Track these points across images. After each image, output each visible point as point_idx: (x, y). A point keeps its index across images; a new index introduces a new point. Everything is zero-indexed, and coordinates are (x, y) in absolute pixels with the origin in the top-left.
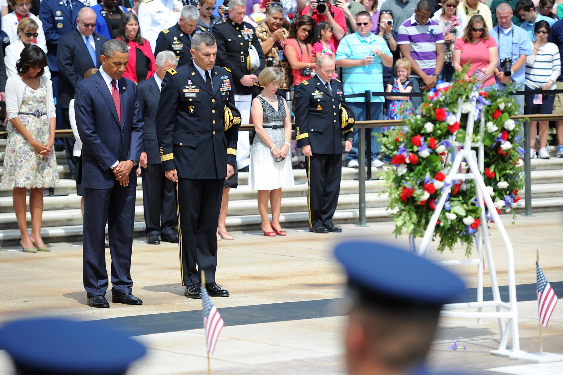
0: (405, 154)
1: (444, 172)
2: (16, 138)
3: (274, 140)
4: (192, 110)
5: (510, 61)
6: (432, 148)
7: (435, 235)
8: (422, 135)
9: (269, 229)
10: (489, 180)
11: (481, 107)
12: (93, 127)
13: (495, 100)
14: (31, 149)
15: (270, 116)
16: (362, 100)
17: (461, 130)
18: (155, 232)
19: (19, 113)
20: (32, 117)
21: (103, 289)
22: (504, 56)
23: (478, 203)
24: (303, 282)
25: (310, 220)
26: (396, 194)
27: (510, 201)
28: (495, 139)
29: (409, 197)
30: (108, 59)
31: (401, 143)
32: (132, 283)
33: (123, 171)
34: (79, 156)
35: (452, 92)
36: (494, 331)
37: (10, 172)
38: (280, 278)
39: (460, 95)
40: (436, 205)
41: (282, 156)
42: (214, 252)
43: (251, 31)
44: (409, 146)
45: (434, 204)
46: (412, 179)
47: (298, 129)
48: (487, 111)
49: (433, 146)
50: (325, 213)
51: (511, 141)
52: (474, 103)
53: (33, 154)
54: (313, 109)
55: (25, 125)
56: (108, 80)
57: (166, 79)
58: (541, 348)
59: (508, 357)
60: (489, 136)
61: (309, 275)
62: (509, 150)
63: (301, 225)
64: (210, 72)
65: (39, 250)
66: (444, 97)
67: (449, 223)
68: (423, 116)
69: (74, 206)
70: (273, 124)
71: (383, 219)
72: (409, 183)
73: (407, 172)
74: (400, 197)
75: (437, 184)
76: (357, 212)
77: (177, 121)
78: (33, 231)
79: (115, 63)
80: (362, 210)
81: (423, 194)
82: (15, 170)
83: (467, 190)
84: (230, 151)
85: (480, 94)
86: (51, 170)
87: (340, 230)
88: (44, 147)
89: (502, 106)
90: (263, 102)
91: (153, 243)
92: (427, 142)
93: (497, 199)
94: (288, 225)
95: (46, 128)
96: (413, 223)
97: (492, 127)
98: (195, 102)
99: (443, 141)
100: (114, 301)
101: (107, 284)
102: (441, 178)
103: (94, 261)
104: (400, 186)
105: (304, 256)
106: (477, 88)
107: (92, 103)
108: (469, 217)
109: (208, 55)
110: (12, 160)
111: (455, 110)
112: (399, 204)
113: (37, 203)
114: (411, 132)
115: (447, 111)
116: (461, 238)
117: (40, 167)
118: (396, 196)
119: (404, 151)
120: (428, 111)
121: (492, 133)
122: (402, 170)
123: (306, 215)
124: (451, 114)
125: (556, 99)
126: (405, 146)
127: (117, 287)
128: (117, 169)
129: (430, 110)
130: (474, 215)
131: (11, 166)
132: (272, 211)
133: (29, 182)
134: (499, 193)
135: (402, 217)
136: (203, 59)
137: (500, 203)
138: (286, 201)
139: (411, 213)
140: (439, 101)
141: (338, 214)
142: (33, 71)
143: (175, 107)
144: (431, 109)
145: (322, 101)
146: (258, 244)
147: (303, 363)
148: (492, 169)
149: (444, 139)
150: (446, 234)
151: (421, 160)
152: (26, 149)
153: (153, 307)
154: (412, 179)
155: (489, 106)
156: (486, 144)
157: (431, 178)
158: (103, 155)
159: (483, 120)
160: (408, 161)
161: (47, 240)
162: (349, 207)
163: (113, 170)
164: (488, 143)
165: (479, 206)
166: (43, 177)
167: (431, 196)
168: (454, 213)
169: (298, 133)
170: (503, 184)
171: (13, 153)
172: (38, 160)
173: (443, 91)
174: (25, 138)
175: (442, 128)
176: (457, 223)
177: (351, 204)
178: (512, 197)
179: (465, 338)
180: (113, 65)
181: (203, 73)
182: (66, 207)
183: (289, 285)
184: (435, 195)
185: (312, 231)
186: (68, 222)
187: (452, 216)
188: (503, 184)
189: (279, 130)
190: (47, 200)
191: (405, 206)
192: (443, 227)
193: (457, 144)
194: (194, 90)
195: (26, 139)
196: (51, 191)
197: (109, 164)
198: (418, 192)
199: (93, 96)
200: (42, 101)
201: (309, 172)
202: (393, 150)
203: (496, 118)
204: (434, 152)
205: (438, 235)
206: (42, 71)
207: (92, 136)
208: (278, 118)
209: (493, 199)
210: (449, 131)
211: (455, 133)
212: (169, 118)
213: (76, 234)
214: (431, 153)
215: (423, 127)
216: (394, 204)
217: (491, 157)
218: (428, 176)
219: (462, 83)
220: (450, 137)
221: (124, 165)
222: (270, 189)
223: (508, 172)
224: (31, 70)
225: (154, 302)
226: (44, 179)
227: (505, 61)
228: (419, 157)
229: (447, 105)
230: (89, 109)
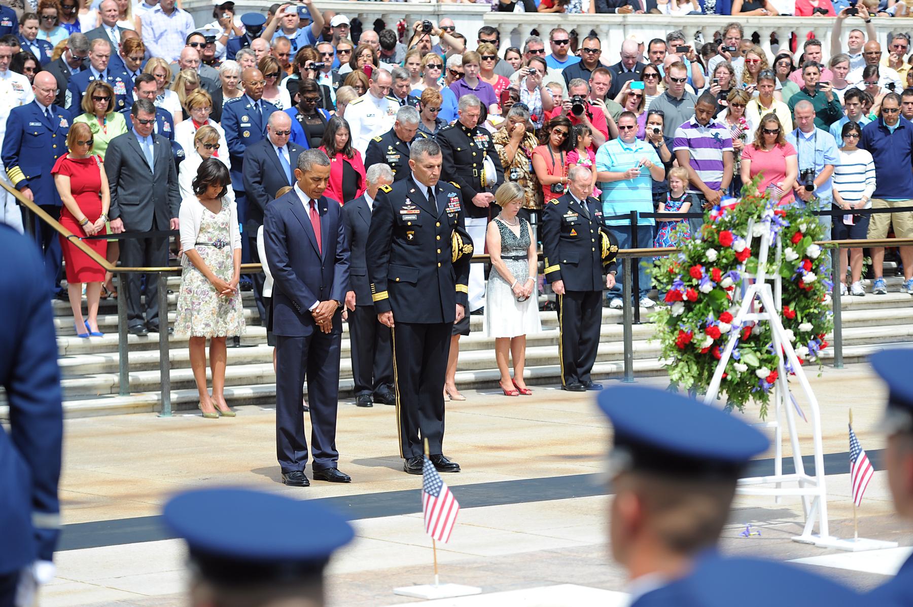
0: (681, 289)
1: (731, 311)
3: (515, 274)
4: (411, 237)
5: (813, 173)
6: (716, 281)
7: (721, 392)
8: (703, 264)
9: (509, 387)
10: (789, 322)
11: (777, 229)
12: (286, 259)
13: (795, 220)
15: (510, 244)
16: (626, 222)
17: (752, 258)
18: (366, 392)
19: (196, 244)
20: (213, 248)
21: (301, 462)
22: (804, 166)
23: (775, 351)
24: (554, 453)
25: (562, 375)
26: (671, 340)
27: (815, 348)
28: (795, 270)
29: (687, 343)
30: (304, 174)
31: (676, 274)
32: (337, 455)
33: (324, 314)
34: (270, 296)
35: (740, 210)
36: (796, 513)
37: (185, 318)
38: (524, 447)
39: (751, 214)
40: (721, 353)
41: (526, 294)
42: (439, 413)
44: (687, 279)
45: (719, 352)
46: (690, 320)
47: (546, 259)
48: (785, 234)
49: (717, 278)
50: (581, 365)
51: (815, 272)
52: (768, 224)
53: (213, 294)
56: (304, 200)
57: (379, 198)
58: (856, 535)
59: (814, 544)
60: (788, 265)
61: (561, 444)
62: (813, 283)
63: (551, 381)
64: (433, 188)
65: (222, 415)
66: (730, 217)
67: (739, 376)
68: (704, 241)
69: (265, 359)
70: (513, 254)
71: (655, 373)
72: (688, 325)
73: (684, 312)
74: (676, 343)
75: (723, 327)
76: (622, 364)
77: (392, 250)
78: (215, 391)
79: (313, 179)
80: (628, 362)
81: (705, 340)
82: (192, 315)
83: (761, 333)
84: (460, 288)
85: (776, 213)
86: (235, 314)
88: (228, 286)
89: (803, 228)
90: (502, 227)
91: (365, 405)
92: (709, 275)
93: (799, 345)
94: (534, 381)
95: (229, 262)
96: (693, 376)
97: (791, 254)
98: (415, 226)
99: (729, 272)
100: (316, 478)
101: (306, 457)
102: (728, 319)
103: (290, 427)
104: (675, 329)
105: (556, 421)
106: (772, 205)
107: (285, 229)
108: (764, 368)
109: (431, 167)
111: (745, 234)
112: (675, 352)
113: (219, 355)
114: (689, 260)
115: (734, 234)
116: (754, 395)
117: (223, 311)
118: (671, 342)
119: (680, 285)
120: (710, 235)
121: (791, 262)
122: (678, 309)
123: (557, 369)
124: (739, 238)
125: (871, 220)
126: (680, 279)
127: (319, 461)
128: (318, 311)
129: (712, 233)
130: (769, 366)
132: (514, 364)
133: (209, 329)
134: (802, 338)
135: (678, 369)
136: (425, 172)
137: (803, 350)
138: (531, 352)
139: (689, 363)
140: (723, 222)
141: (597, 368)
142: (212, 191)
143: (390, 232)
144: (715, 231)
145: (577, 225)
147: (555, 555)
148: (792, 308)
149: (731, 269)
150: (734, 390)
151: (702, 297)
153: (364, 485)
154: (690, 320)
155: (787, 228)
156: (784, 276)
157: (715, 319)
158: (299, 293)
159: (779, 245)
160: (685, 298)
161: (232, 402)
162: (611, 358)
163: (312, 312)
164: (786, 274)
165: (776, 354)
166: (226, 323)
167: (714, 341)
168: (745, 363)
169: (547, 265)
170: (806, 327)
173: (729, 209)
174: (204, 275)
175: (729, 256)
176: (749, 376)
177: (614, 354)
178: (817, 343)
179: (760, 521)
180: (311, 181)
181: (424, 190)
182: (255, 361)
183: (536, 457)
184: (720, 341)
186: (258, 380)
187: (742, 368)
188: (806, 327)
189: (521, 262)
190: (232, 352)
191: (682, 355)
192: (731, 381)
193: (747, 276)
194: (413, 212)
196: (236, 341)
197: (306, 305)
198: (698, 336)
199: (286, 220)
200: (225, 228)
201: (561, 315)
202: (667, 284)
203: (796, 243)
204: (718, 287)
205: (724, 391)
206: (224, 191)
207: (286, 271)
208: (520, 246)
209: (794, 345)
210: (737, 259)
211: (744, 262)
212: (382, 247)
213: (268, 394)
214: (714, 288)
215: (704, 254)
216: (668, 352)
217: (791, 291)
218: (711, 316)
219: (753, 199)
220: (738, 266)
221: (326, 306)
222: (511, 336)
223: (812, 310)
224: (211, 190)
225: (366, 479)
227: (806, 173)
228: (700, 292)
229: (735, 226)
230: (281, 236)
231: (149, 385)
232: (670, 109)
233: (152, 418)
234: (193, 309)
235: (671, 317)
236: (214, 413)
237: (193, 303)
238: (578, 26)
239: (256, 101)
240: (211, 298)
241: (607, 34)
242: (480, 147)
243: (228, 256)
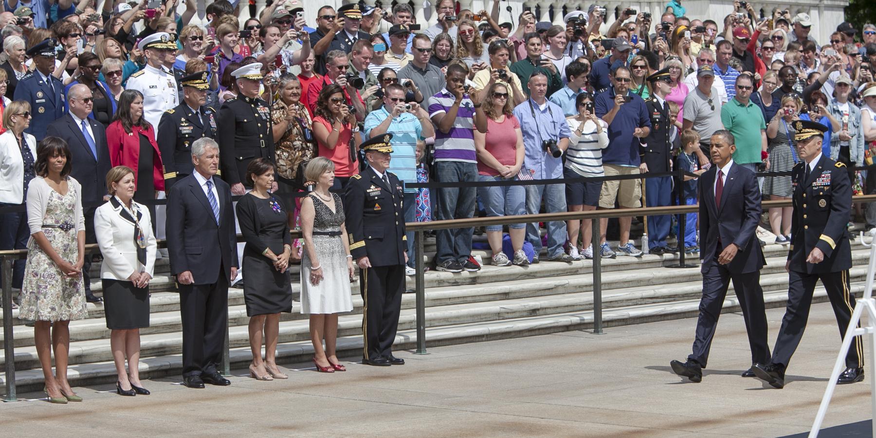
2: (40, 258)
9: (325, 363)
14: (57, 271)
15: (328, 220)
19: (43, 226)
20: (59, 230)
37: (30, 301)
43: (267, 110)
54: (370, 210)
55: (51, 241)
65: (69, 400)
69: (79, 337)
70: (330, 230)
71: (437, 343)
82: (37, 298)
86: (80, 298)
87: (400, 362)
88: (73, 268)
90: (317, 202)
110: (33, 286)
125: (603, 186)
131: (30, 293)
145: (381, 198)
146: (328, 384)
152: (52, 272)
166: (69, 307)
171: (34, 276)
172: (64, 286)
185: (368, 364)
195: (53, 259)
208: (336, 222)
222: (327, 312)
226: (71, 310)
234: (39, 292)
237: (39, 287)
240: (57, 281)
243: (73, 239)
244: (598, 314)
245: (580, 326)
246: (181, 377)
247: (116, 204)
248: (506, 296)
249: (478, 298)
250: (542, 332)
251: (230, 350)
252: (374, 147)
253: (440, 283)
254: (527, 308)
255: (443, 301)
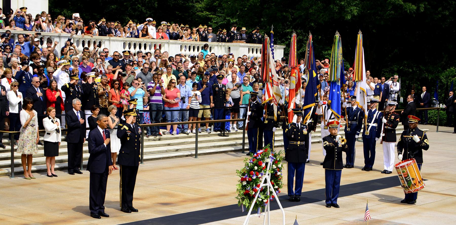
5: (185, 98)
6: (257, 175)
20: (31, 126)
22: (182, 96)
24: (157, 202)
37: (21, 148)
60: (273, 170)
65: (31, 178)
69: (35, 156)
75: (257, 188)
82: (23, 147)
90: (112, 119)
97: (274, 167)
102: (258, 186)
107: (95, 140)
121: (274, 169)
122: (245, 183)
133: (29, 152)
135: (245, 201)
160: (247, 180)
168: (261, 198)
184: (256, 192)
188: (276, 187)
198: (251, 192)
215: (254, 168)
218: (254, 186)
231: (2, 166)
232: (143, 76)
233: (7, 178)
234: (24, 146)
235: (242, 185)
236: (30, 178)
237: (24, 144)
238: (96, 40)
239: (27, 72)
241: (104, 42)
242: (96, 89)
244: (196, 152)
245: (191, 155)
246: (67, 170)
247: (50, 118)
248: (169, 145)
249: (160, 145)
250: (179, 157)
251: (83, 161)
252: (131, 102)
253: (149, 140)
254: (175, 149)
255: (149, 146)
